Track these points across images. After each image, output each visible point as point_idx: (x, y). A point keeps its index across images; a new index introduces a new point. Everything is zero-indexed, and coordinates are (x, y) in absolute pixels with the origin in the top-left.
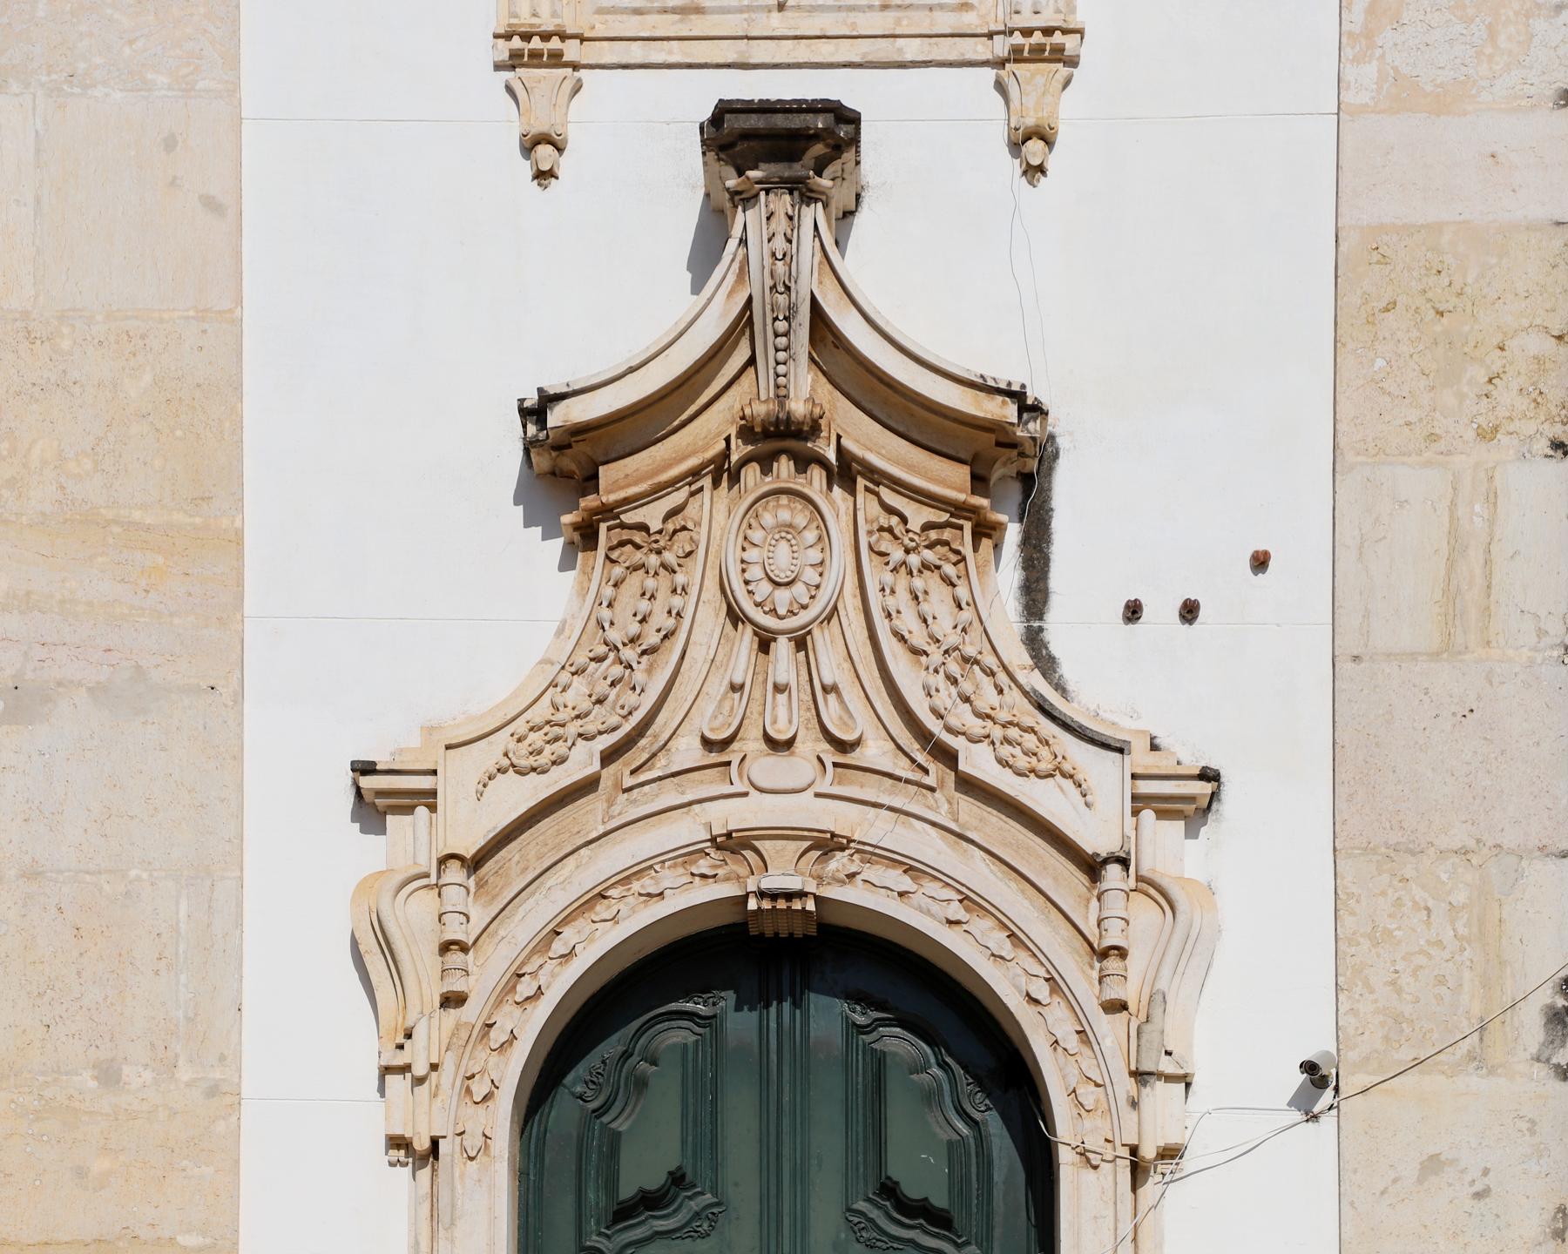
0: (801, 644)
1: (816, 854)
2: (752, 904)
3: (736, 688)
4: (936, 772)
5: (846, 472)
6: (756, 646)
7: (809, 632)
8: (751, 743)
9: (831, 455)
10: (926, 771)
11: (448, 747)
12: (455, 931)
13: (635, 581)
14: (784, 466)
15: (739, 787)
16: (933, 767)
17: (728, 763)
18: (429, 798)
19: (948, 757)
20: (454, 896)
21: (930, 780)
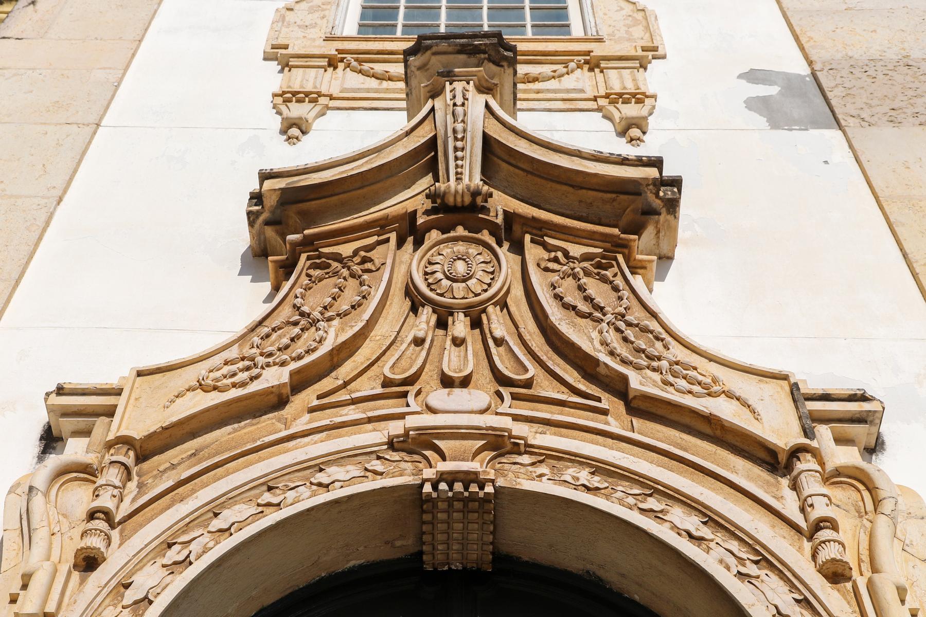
0: (476, 324)
1: (488, 455)
2: (427, 488)
3: (418, 342)
4: (607, 401)
5: (512, 232)
6: (434, 318)
7: (484, 311)
8: (430, 378)
9: (500, 220)
10: (599, 400)
11: (140, 374)
12: (106, 501)
13: (334, 280)
14: (460, 231)
15: (414, 407)
16: (605, 396)
17: (405, 395)
18: (110, 412)
19: (618, 387)
20: (113, 475)
21: (604, 405)
